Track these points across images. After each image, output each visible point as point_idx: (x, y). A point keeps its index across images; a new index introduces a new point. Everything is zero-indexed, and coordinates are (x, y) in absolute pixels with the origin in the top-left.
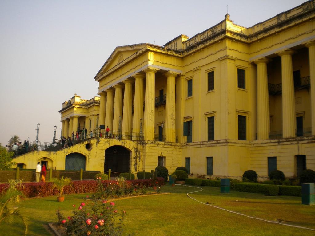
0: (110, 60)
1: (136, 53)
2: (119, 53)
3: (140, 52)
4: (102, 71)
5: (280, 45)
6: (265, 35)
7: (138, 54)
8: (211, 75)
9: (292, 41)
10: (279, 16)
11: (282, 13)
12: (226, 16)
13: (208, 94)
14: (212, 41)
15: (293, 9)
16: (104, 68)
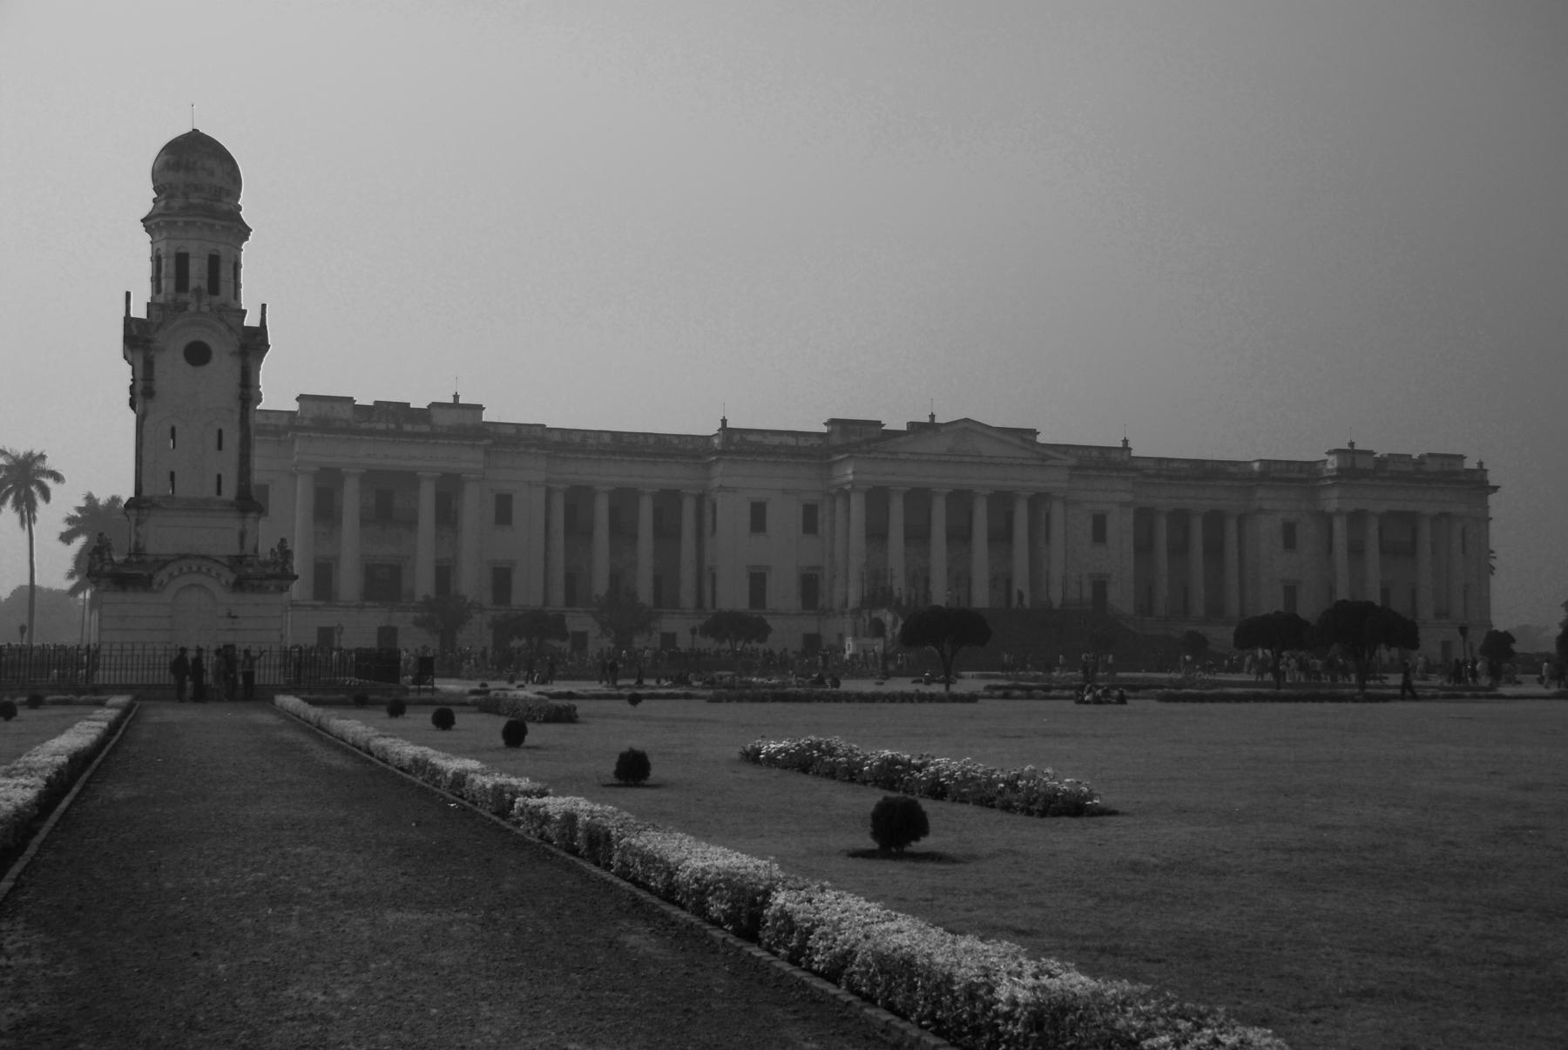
8: (1099, 523)
12: (1125, 441)
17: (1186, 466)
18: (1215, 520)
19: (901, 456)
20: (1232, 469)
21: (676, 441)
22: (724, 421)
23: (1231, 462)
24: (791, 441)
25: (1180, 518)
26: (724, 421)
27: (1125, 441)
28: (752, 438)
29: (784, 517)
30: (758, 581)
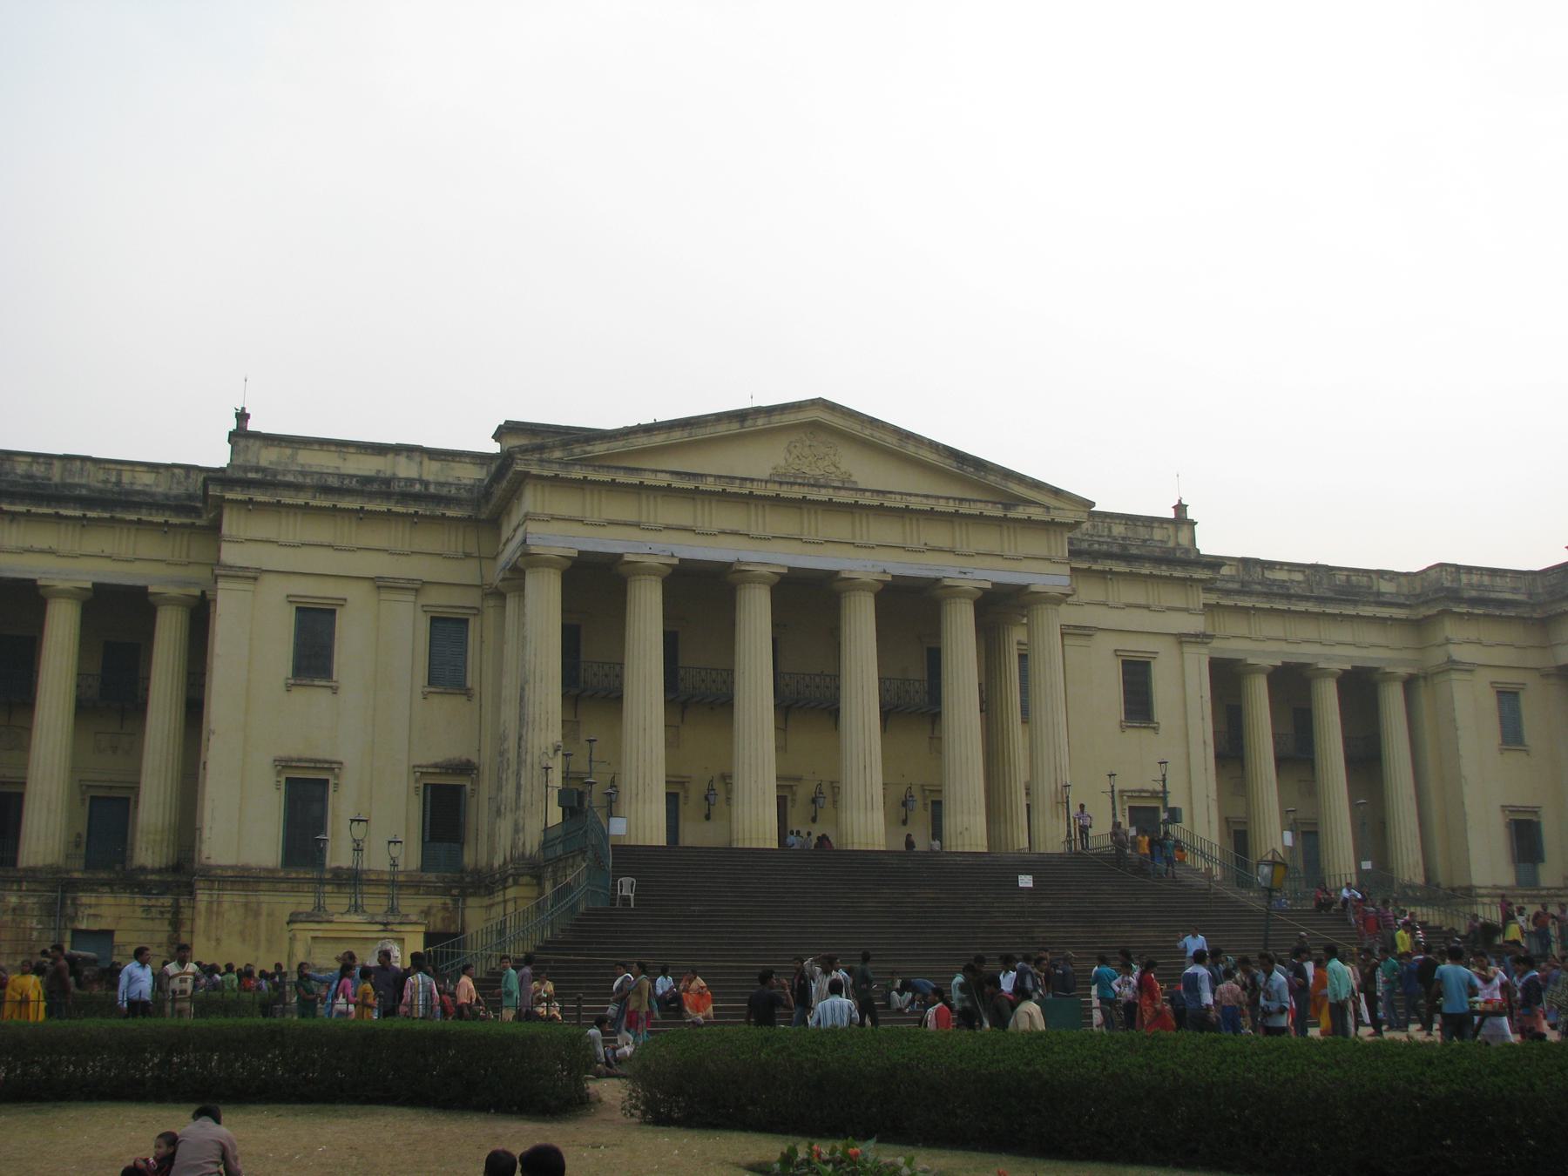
0: (734, 427)
1: (1007, 507)
2: (815, 427)
3: (1036, 513)
4: (618, 446)
5: (1264, 644)
6: (1223, 602)
7: (1011, 514)
8: (1136, 676)
9: (1286, 647)
10: (1246, 563)
11: (1257, 562)
12: (1180, 508)
13: (1129, 731)
14: (1164, 571)
15: (1282, 564)
16: (643, 441)
17: (1298, 577)
18: (1360, 688)
19: (649, 479)
20: (1386, 587)
21: (147, 478)
22: (242, 416)
23: (1381, 574)
24: (405, 469)
25: (1292, 684)
26: (242, 416)
27: (1180, 508)
28: (305, 458)
29: (380, 643)
30: (306, 796)
